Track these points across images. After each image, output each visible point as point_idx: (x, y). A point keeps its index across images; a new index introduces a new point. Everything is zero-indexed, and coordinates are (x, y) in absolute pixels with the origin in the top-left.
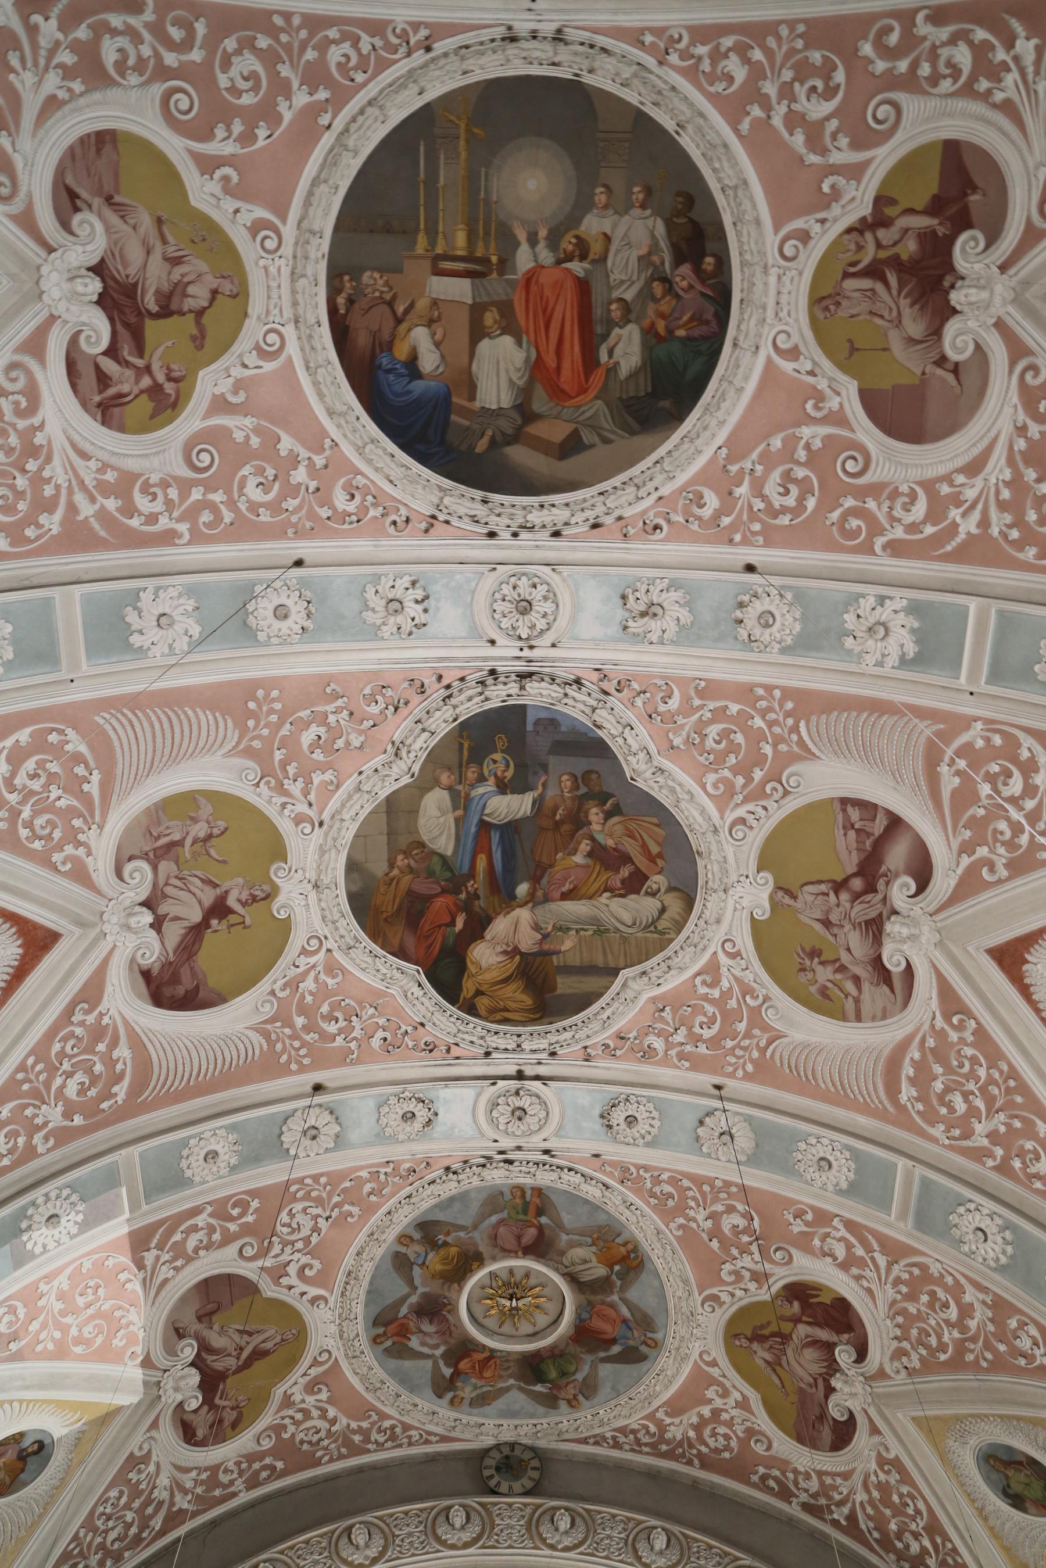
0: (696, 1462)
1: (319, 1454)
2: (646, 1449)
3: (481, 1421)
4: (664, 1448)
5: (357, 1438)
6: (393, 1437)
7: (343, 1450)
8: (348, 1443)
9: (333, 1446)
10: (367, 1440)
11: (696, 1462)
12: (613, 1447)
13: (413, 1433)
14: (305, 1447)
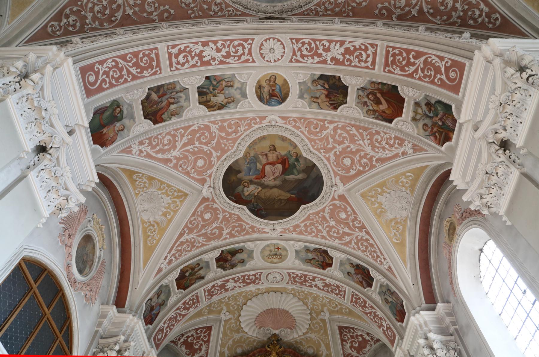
0: (351, 13)
1: (190, 12)
2: (329, 12)
3: (259, 3)
4: (337, 9)
5: (205, 7)
6: (221, 10)
7: (200, 13)
8: (202, 9)
9: (195, 9)
10: (210, 9)
11: (351, 13)
12: (315, 15)
13: (230, 9)
14: (183, 5)
